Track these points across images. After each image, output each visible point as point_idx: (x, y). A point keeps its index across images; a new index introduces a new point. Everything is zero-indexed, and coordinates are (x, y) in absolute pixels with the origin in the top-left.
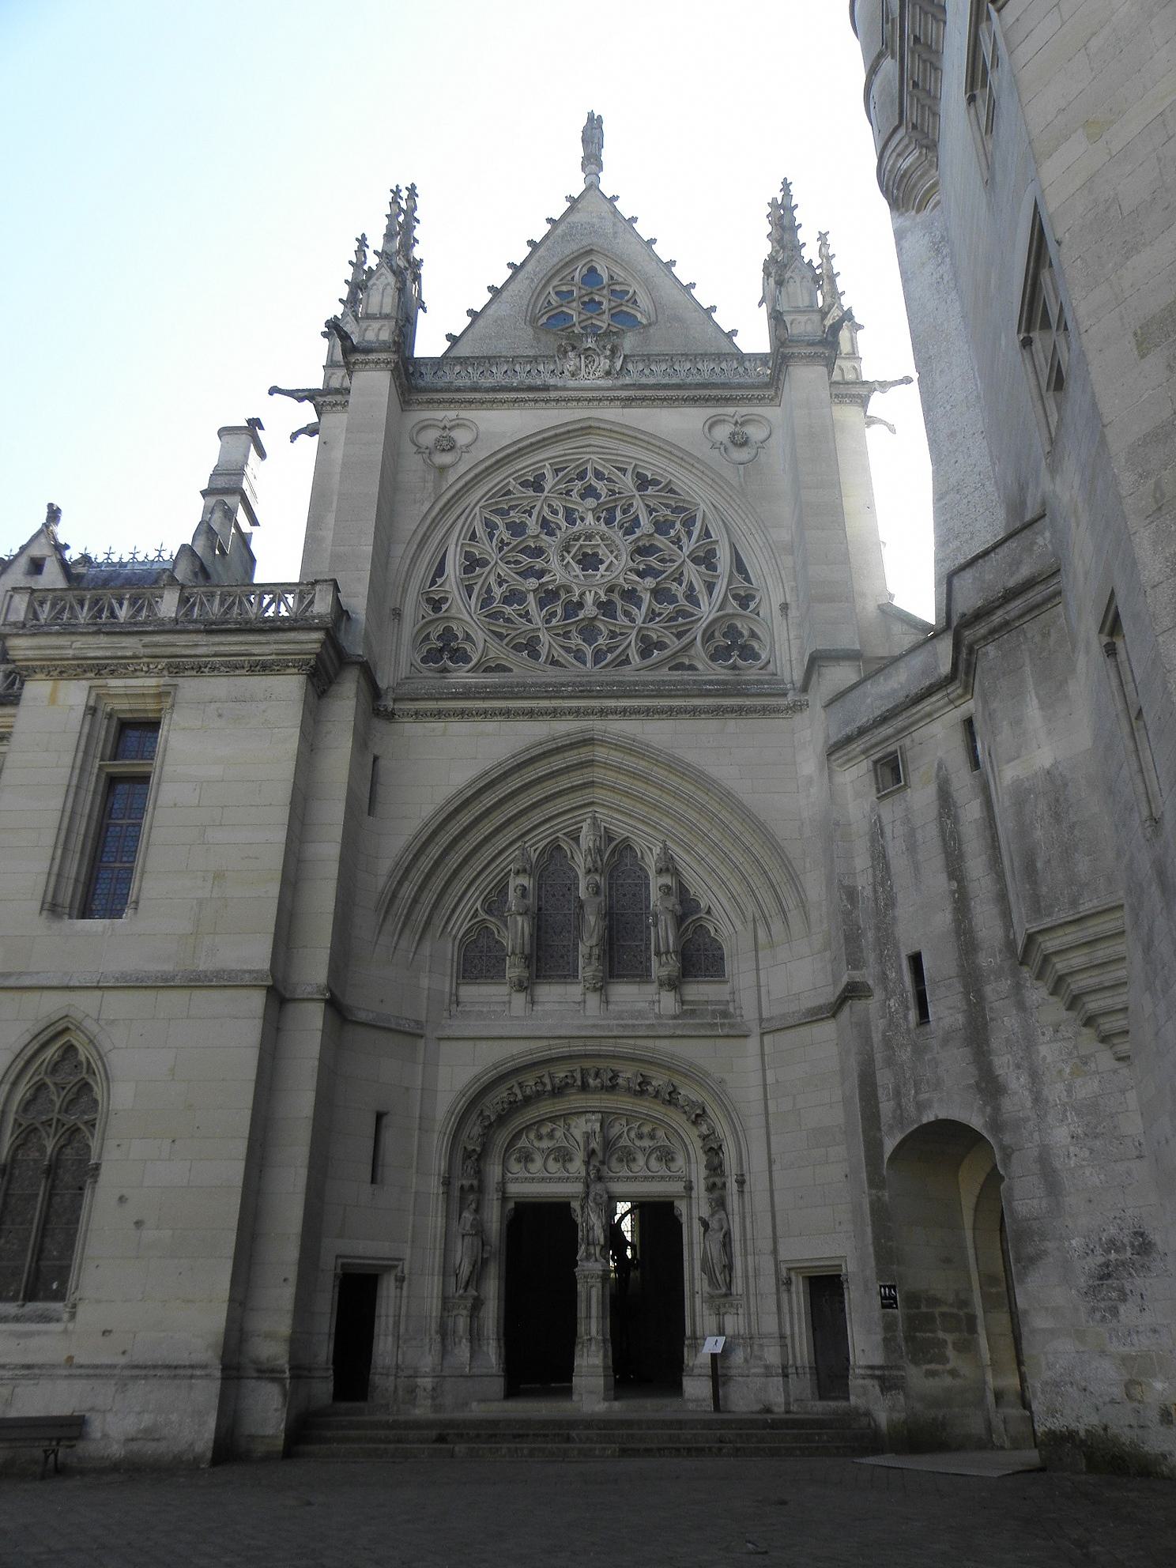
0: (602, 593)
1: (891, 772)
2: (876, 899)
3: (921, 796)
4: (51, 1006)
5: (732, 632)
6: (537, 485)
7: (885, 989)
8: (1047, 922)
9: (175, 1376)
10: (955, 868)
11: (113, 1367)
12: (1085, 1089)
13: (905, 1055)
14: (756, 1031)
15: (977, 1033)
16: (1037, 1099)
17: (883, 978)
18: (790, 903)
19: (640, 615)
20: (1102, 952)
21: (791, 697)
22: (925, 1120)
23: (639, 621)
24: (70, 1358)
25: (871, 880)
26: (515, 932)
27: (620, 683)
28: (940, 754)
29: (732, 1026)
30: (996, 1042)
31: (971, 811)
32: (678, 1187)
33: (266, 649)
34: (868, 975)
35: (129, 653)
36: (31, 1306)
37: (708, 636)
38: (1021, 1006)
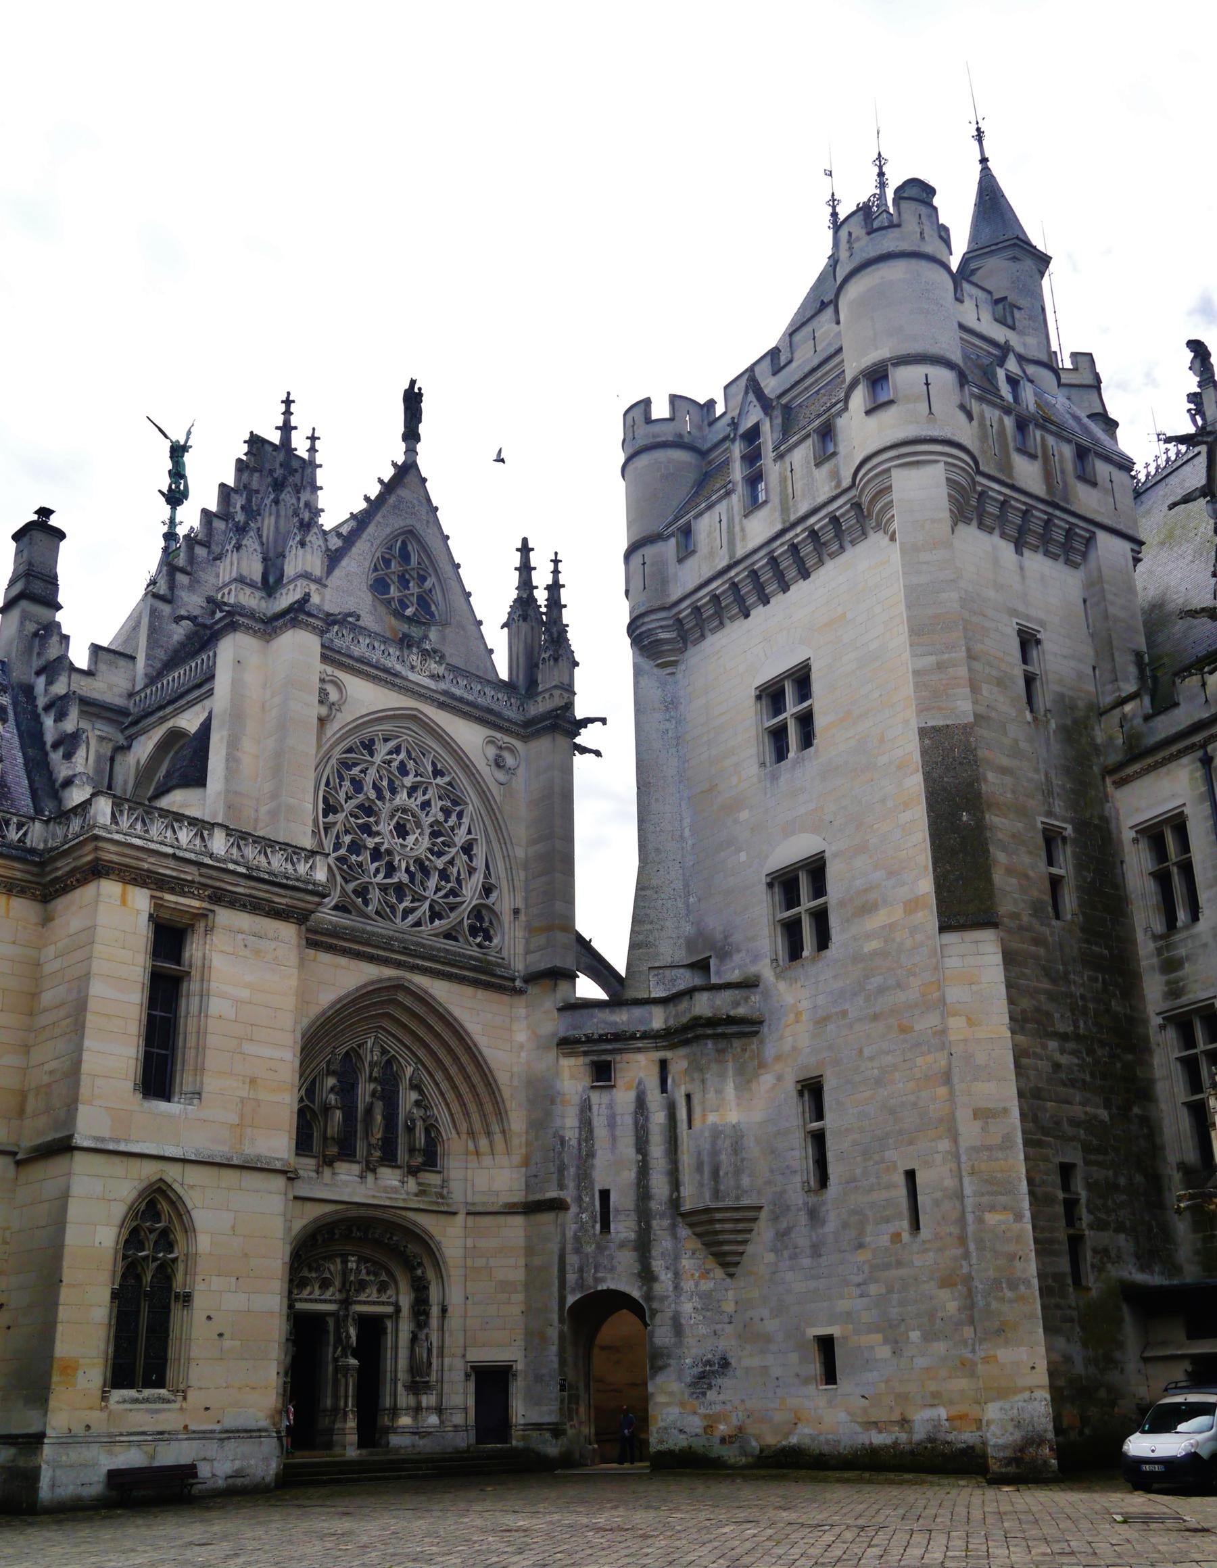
0: (411, 862)
1: (602, 1073)
2: (580, 1149)
3: (624, 1098)
4: (150, 1171)
5: (479, 917)
6: (369, 746)
7: (580, 1207)
8: (720, 1204)
9: (251, 1437)
10: (642, 1146)
11: (212, 1432)
12: (706, 1285)
13: (590, 1249)
14: (463, 1211)
15: (643, 1245)
16: (677, 1287)
17: (579, 1199)
18: (496, 1128)
20: (741, 1226)
21: (518, 983)
22: (599, 1288)
24: (186, 1427)
25: (577, 1135)
27: (423, 945)
28: (642, 1074)
29: (448, 1205)
30: (656, 1252)
31: (658, 1118)
32: (389, 1309)
33: (283, 901)
34: (568, 1195)
35: (189, 878)
36: (147, 1392)
38: (674, 1236)
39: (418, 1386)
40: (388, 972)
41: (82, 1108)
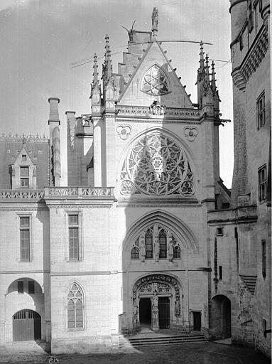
5: (187, 185)
19: (168, 179)
21: (200, 203)
23: (167, 182)
26: (142, 252)
37: (182, 185)
39: (178, 315)
40: (153, 209)
41: (52, 266)
